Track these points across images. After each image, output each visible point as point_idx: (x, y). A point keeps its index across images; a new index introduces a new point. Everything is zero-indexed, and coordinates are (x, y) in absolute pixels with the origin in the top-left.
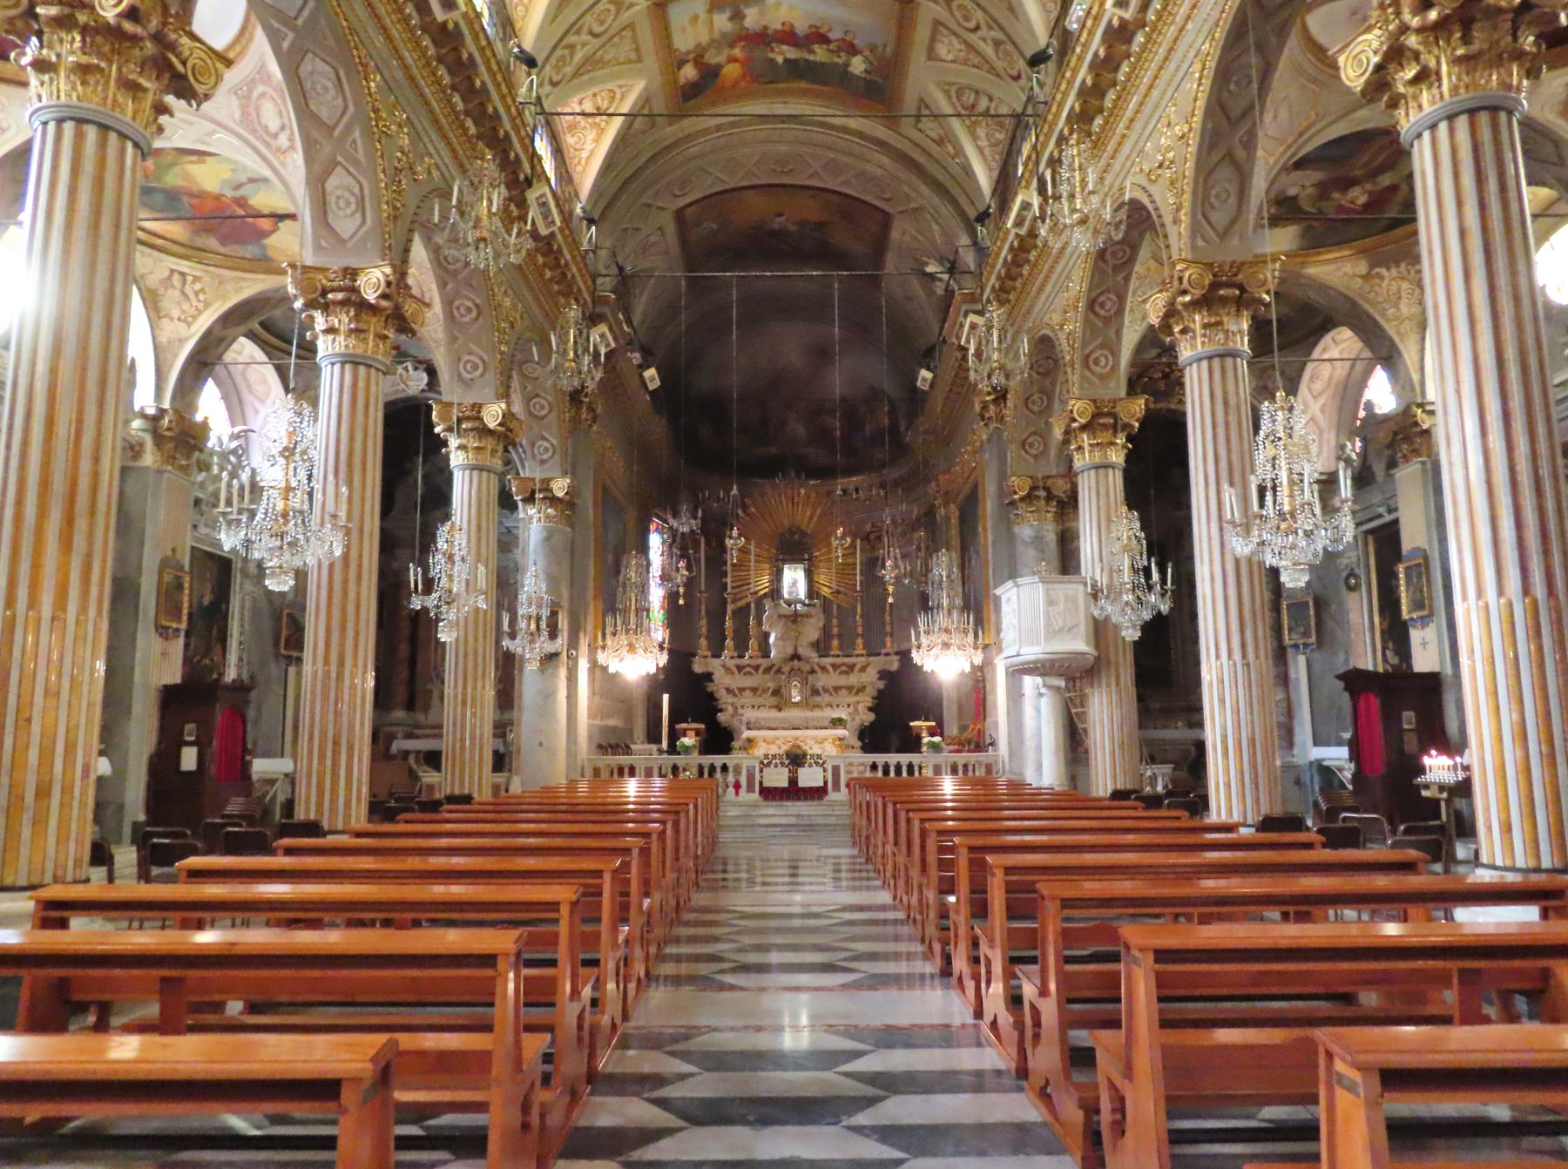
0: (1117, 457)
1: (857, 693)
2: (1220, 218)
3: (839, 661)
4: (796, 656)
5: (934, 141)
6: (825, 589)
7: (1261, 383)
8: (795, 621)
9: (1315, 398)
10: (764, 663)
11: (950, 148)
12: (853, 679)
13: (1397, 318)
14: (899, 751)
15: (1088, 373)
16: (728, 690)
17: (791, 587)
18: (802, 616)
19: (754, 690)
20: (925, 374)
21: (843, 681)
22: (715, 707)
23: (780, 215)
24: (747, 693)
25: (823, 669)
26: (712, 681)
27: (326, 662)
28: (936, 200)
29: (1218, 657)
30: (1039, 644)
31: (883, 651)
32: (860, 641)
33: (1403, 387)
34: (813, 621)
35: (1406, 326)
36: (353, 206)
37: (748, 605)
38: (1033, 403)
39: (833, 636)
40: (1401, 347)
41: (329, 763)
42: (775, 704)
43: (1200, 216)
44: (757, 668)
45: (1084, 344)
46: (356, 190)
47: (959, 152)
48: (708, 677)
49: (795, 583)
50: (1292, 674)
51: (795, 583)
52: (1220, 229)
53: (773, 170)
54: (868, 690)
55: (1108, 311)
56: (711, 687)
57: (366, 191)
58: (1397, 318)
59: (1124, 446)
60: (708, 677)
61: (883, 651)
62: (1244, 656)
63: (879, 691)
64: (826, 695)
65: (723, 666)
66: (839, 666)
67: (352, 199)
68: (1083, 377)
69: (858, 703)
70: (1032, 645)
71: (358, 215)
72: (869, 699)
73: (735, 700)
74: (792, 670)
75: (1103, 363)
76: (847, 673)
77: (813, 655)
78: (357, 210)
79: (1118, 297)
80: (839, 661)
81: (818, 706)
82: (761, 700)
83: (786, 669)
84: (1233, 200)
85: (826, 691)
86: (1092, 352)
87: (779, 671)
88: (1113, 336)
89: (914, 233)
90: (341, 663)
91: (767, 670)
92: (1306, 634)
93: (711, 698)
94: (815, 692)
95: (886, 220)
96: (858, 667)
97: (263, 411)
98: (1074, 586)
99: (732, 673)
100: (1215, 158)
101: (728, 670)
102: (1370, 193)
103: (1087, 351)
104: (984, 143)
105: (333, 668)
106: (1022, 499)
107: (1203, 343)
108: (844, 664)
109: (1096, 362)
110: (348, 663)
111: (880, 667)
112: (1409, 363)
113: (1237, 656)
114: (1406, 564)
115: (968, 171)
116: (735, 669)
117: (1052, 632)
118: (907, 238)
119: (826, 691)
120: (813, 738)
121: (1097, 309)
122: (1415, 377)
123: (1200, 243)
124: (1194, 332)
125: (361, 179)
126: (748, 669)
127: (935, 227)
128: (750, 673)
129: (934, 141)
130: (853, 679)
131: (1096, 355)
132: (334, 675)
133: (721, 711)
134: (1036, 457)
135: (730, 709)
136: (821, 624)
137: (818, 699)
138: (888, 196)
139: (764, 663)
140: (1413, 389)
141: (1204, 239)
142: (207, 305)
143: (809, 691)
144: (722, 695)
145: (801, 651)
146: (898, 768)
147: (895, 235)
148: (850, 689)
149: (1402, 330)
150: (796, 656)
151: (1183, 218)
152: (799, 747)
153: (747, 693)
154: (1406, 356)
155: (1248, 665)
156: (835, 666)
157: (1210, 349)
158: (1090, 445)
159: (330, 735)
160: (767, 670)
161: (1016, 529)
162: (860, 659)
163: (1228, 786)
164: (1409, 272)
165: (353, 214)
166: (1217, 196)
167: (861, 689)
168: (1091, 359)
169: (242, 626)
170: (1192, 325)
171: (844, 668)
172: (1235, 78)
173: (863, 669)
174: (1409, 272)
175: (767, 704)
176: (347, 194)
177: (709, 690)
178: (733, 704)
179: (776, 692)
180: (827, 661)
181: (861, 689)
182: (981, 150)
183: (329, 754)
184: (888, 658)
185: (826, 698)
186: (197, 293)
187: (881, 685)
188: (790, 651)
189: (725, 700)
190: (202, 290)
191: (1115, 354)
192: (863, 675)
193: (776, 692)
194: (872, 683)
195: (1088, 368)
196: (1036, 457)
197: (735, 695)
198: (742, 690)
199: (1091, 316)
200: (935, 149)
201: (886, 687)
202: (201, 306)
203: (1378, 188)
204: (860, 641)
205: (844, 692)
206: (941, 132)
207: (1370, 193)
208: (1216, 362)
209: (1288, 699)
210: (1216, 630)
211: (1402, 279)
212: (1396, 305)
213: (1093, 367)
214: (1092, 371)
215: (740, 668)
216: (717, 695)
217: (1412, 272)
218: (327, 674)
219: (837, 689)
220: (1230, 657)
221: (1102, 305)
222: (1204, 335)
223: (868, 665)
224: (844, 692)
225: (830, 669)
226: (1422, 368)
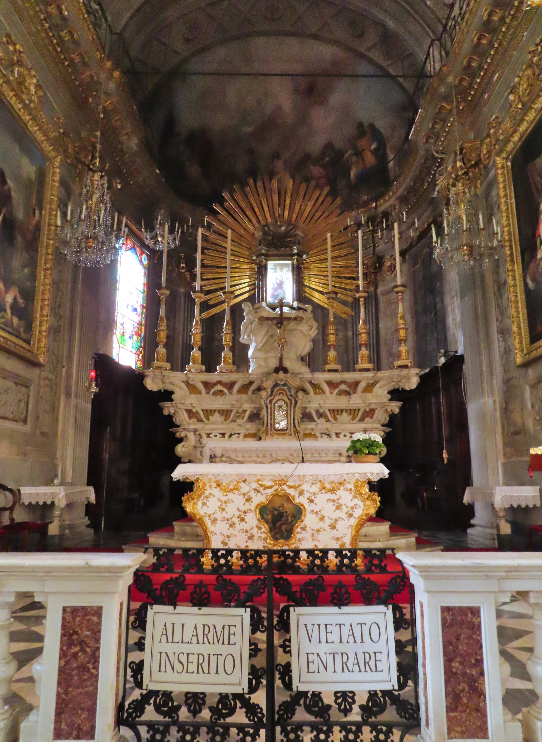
1: (362, 420)
3: (335, 377)
4: (281, 368)
6: (317, 295)
10: (240, 379)
16: (191, 413)
17: (275, 289)
18: (289, 319)
19: (225, 413)
21: (342, 402)
22: (174, 434)
24: (216, 417)
25: (316, 387)
34: (303, 327)
37: (225, 309)
39: (329, 346)
42: (252, 431)
44: (230, 386)
48: (167, 395)
49: (280, 285)
51: (280, 285)
56: (168, 409)
60: (167, 395)
61: (397, 363)
63: (392, 416)
64: (322, 420)
65: (187, 384)
73: (199, 426)
74: (276, 385)
76: (348, 393)
77: (305, 371)
80: (335, 377)
81: (310, 435)
82: (234, 427)
83: (268, 384)
85: (321, 415)
87: (259, 389)
91: (244, 389)
93: (170, 421)
94: (307, 417)
96: (362, 385)
101: (192, 388)
108: (343, 382)
111: (391, 387)
116: (201, 387)
119: (321, 415)
120: (316, 480)
126: (219, 387)
128: (221, 392)
133: (181, 440)
135: (192, 437)
136: (313, 333)
137: (312, 425)
139: (240, 379)
143: (299, 415)
144: (181, 418)
145: (287, 364)
148: (353, 412)
150: (281, 368)
152: (287, 498)
153: (216, 417)
156: (332, 385)
160: (244, 389)
167: (370, 413)
171: (343, 387)
173: (369, 388)
175: (243, 432)
177: (166, 412)
178: (195, 431)
179: (255, 417)
180: (321, 377)
181: (370, 413)
184: (405, 372)
185: (321, 425)
187: (395, 407)
188: (274, 363)
192: (369, 395)
193: (255, 417)
194: (383, 405)
197: (200, 421)
198: (208, 413)
201: (402, 409)
204: (364, 352)
205: (345, 416)
215: (207, 385)
216: (177, 420)
219: (336, 412)
223: (376, 382)
224: (345, 416)
225: (326, 388)
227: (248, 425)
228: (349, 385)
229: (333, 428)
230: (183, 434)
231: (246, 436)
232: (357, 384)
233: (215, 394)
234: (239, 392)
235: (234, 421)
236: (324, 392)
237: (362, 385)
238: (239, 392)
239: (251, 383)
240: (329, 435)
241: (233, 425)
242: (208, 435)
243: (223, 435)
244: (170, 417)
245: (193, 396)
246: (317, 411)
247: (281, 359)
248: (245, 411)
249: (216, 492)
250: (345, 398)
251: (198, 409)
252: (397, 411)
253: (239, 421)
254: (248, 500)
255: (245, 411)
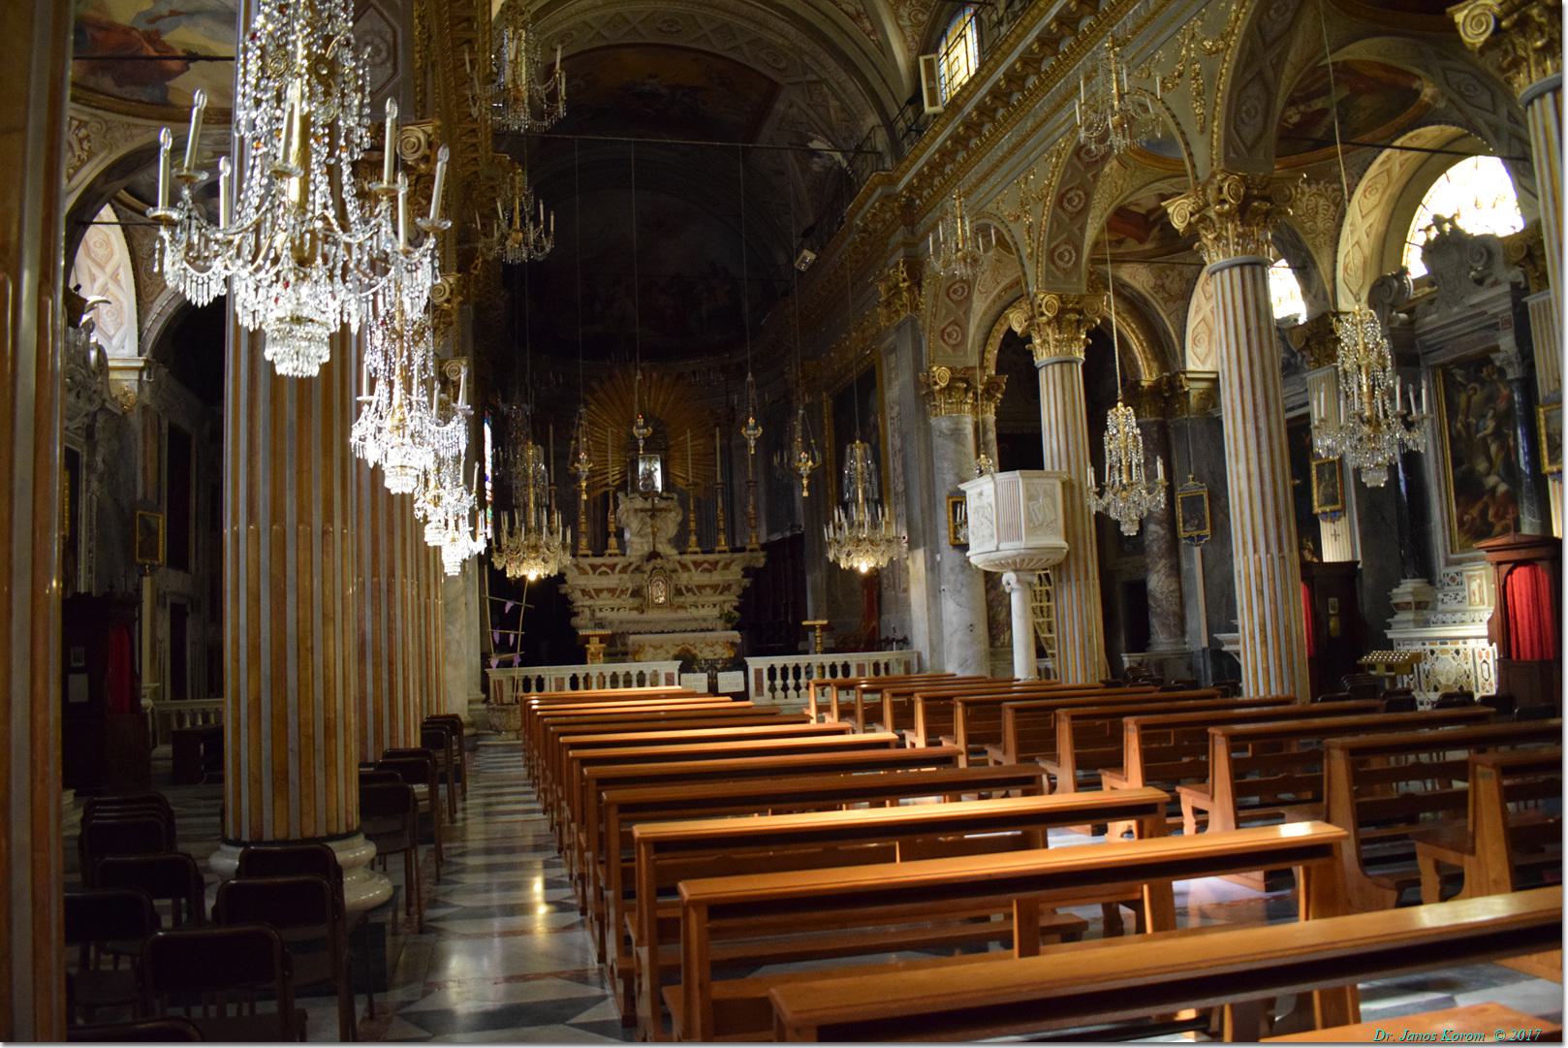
0: (1080, 355)
1: (721, 593)
2: (1249, 133)
3: (700, 557)
4: (654, 555)
5: (847, 13)
6: (679, 480)
7: (1159, 282)
8: (652, 517)
9: (1207, 299)
10: (621, 561)
11: (867, 25)
12: (716, 577)
13: (1313, 231)
14: (827, 651)
15: (1052, 267)
16: (584, 592)
17: (644, 479)
18: (661, 510)
19: (612, 591)
20: (810, 256)
23: (651, 76)
24: (605, 594)
25: (685, 567)
26: (565, 582)
27: (375, 573)
28: (843, 76)
29: (1255, 551)
30: (1019, 538)
31: (717, 549)
32: (722, 537)
33: (1315, 297)
34: (673, 514)
35: (1321, 239)
36: (384, 54)
38: (955, 292)
39: (690, 532)
40: (1316, 257)
41: (385, 685)
42: (636, 605)
43: (1233, 131)
44: (613, 567)
45: (1051, 239)
46: (389, 37)
47: (878, 28)
50: (1185, 565)
52: (1249, 144)
53: (660, 30)
54: (734, 588)
55: (1075, 207)
56: (564, 589)
57: (400, 40)
58: (1313, 231)
59: (1085, 341)
62: (1281, 549)
63: (745, 589)
66: (702, 563)
67: (383, 47)
68: (1048, 272)
69: (724, 602)
70: (1010, 539)
71: (389, 65)
72: (734, 598)
74: (654, 568)
75: (1066, 259)
76: (710, 571)
78: (387, 59)
79: (1085, 194)
80: (700, 557)
81: (682, 607)
84: (1259, 118)
85: (689, 590)
86: (1057, 247)
88: (1077, 232)
89: (803, 105)
90: (391, 574)
91: (624, 570)
92: (1201, 526)
94: (679, 592)
95: (774, 89)
96: (721, 564)
97: (101, 280)
98: (1051, 481)
99: (586, 573)
100: (1249, 76)
102: (1303, 114)
103: (1052, 246)
104: (905, 23)
105: (383, 580)
106: (942, 390)
107: (1236, 251)
108: (705, 561)
109: (1061, 256)
110: (399, 572)
111: (744, 564)
112: (1322, 272)
113: (1274, 549)
114: (1318, 462)
115: (885, 49)
116: (589, 569)
117: (1033, 528)
118: (795, 110)
119: (689, 590)
121: (1066, 205)
122: (1328, 288)
123: (1232, 155)
124: (1227, 239)
125: (395, 24)
126: (603, 569)
127: (833, 103)
128: (605, 573)
129: (847, 13)
130: (716, 577)
131: (1061, 249)
132: (384, 587)
133: (576, 614)
134: (954, 347)
136: (679, 518)
137: (682, 599)
138: (782, 66)
139: (621, 561)
140: (1325, 298)
141: (1235, 152)
142: (91, 155)
144: (577, 594)
146: (833, 668)
147: (780, 106)
148: (714, 587)
149: (1318, 243)
151: (1215, 129)
152: (688, 651)
154: (1320, 267)
155: (1283, 557)
156: (697, 564)
157: (1241, 258)
158: (1056, 340)
159: (385, 653)
160: (624, 570)
161: (933, 421)
162: (724, 555)
163: (1267, 671)
164: (1326, 189)
165: (383, 63)
166: (1248, 112)
168: (1056, 254)
169: (91, 530)
170: (1224, 233)
171: (706, 565)
172: (1275, 5)
173: (727, 566)
174: (1326, 189)
176: (377, 41)
177: (562, 591)
178: (589, 607)
179: (637, 593)
180: (688, 558)
181: (727, 588)
182: (901, 29)
183: (385, 676)
184: (755, 554)
185: (690, 598)
186: (81, 141)
187: (747, 582)
188: (647, 549)
189: (580, 601)
190: (87, 137)
191: (1078, 250)
193: (637, 593)
195: (1053, 262)
196: (954, 347)
197: (591, 597)
198: (598, 591)
199: (1059, 210)
200: (849, 24)
201: (752, 583)
202: (84, 156)
203: (1309, 110)
204: (722, 537)
206: (860, 7)
207: (1303, 114)
208: (1247, 270)
209: (1180, 589)
210: (1253, 525)
211: (1320, 195)
212: (1313, 219)
213: (1058, 261)
214: (1057, 267)
215: (594, 568)
217: (1329, 189)
218: (376, 587)
219: (701, 588)
220: (1268, 551)
221: (1070, 201)
222: (1238, 244)
223: (733, 561)
225: (692, 567)
226: (1334, 279)
227: (631, 601)
228: (710, 563)
229: (701, 600)
230: (580, 609)
231: (630, 609)
232: (717, 562)
233: (600, 574)
234: (620, 572)
235: (619, 597)
236: (689, 570)
237: (721, 564)
238: (620, 572)
239: (630, 564)
240: (697, 607)
241: (619, 601)
242: (601, 610)
243: (613, 609)
244: (566, 595)
245: (583, 577)
246: (686, 587)
247: (654, 547)
248: (627, 589)
249: (651, 649)
250: (708, 575)
251: (590, 588)
252: (748, 585)
253: (623, 597)
254: (668, 653)
255: (627, 589)
